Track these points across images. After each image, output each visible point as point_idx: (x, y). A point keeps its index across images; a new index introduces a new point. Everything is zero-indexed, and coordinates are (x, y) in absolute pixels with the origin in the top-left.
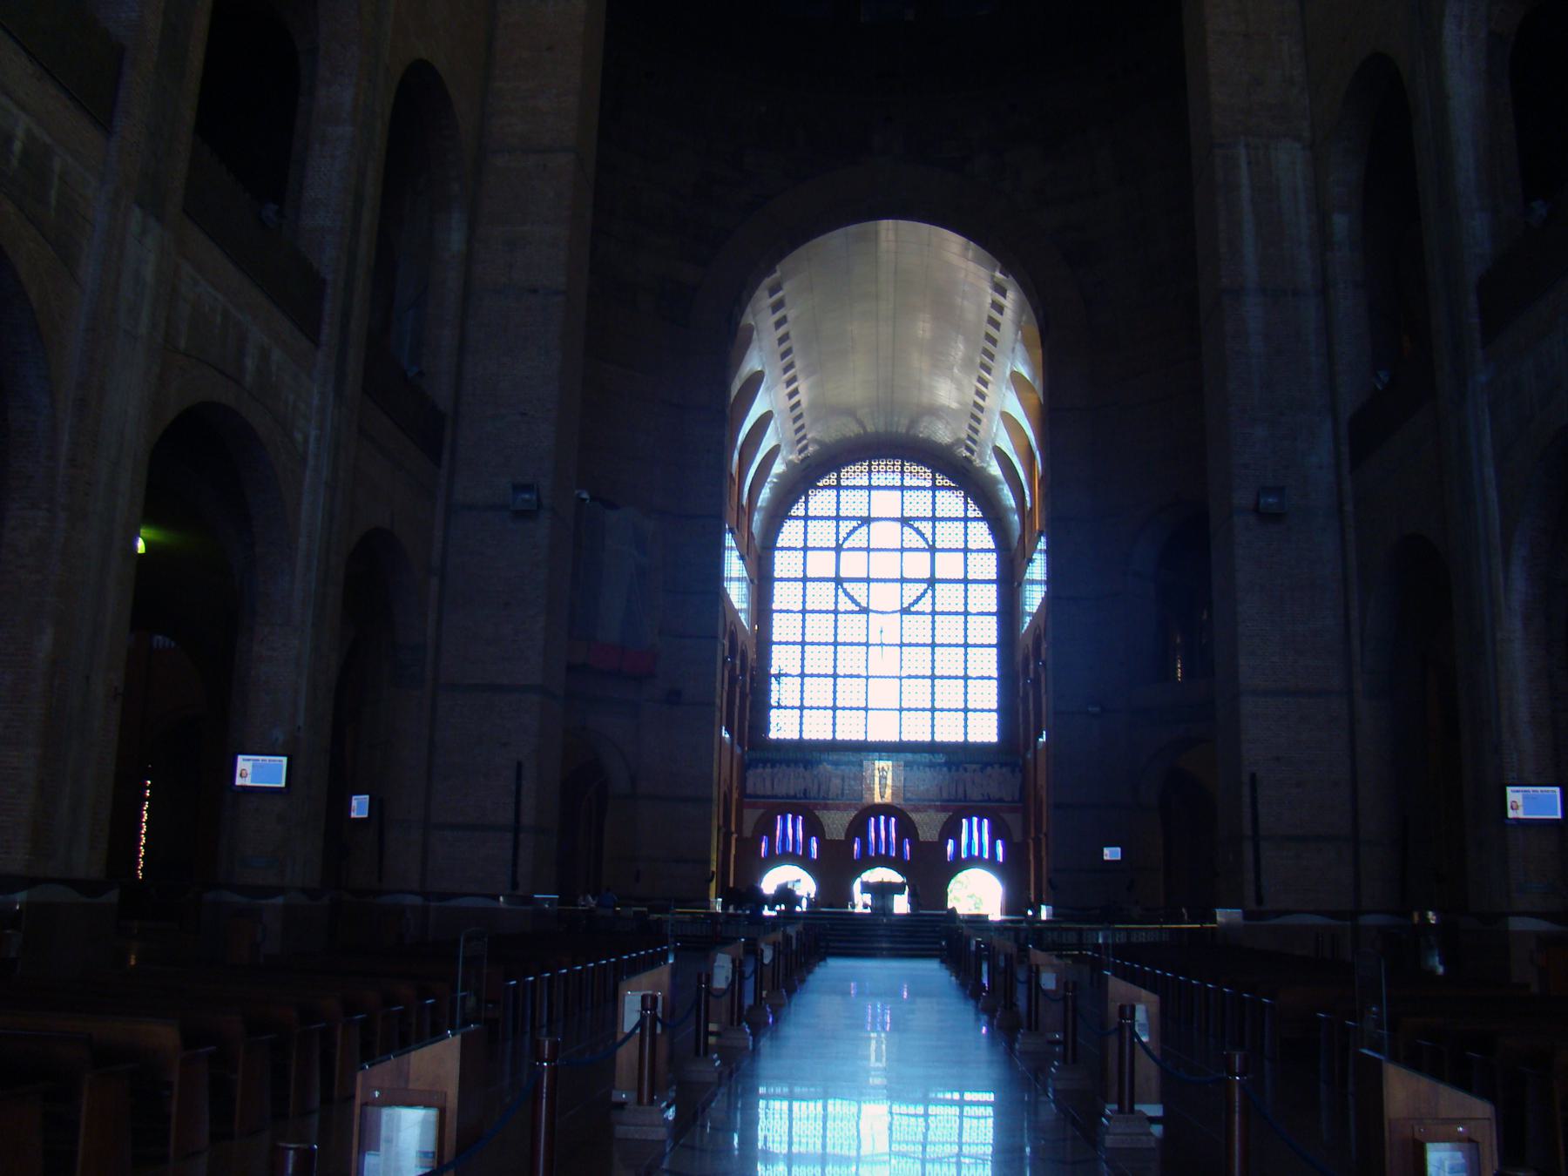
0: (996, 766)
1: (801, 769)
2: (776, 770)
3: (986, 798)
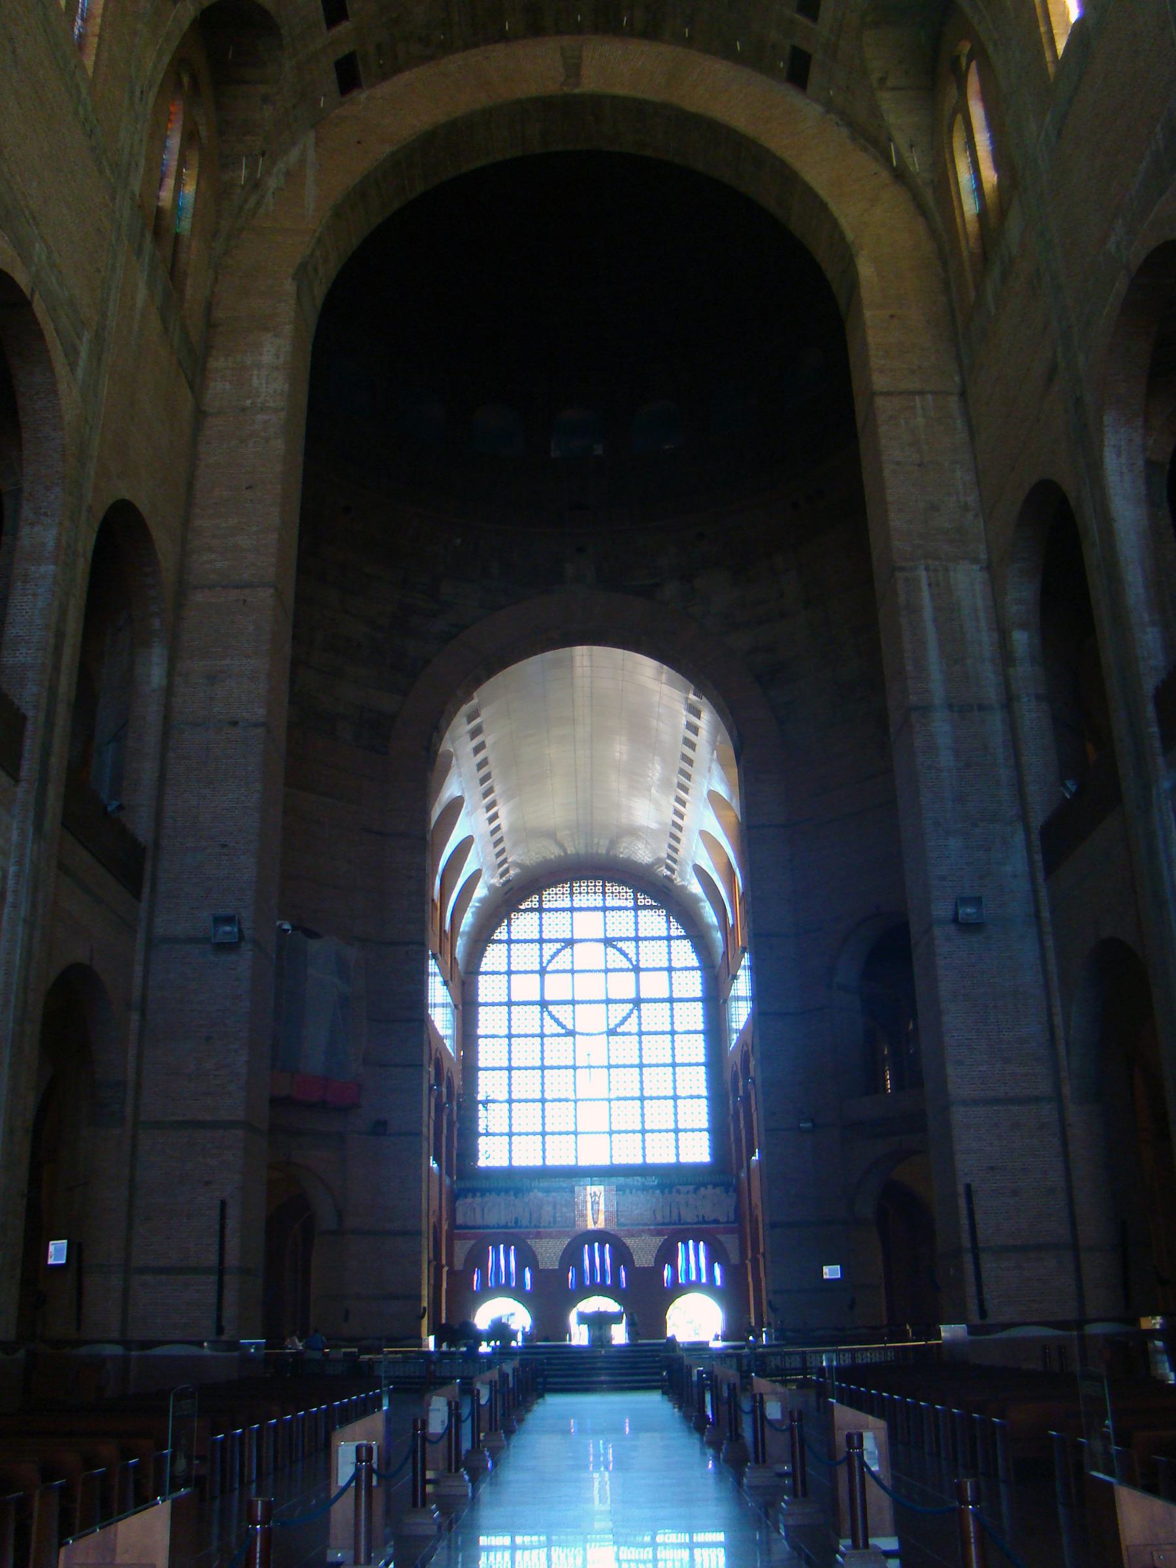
0: (710, 1187)
2: (485, 1199)
3: (701, 1218)
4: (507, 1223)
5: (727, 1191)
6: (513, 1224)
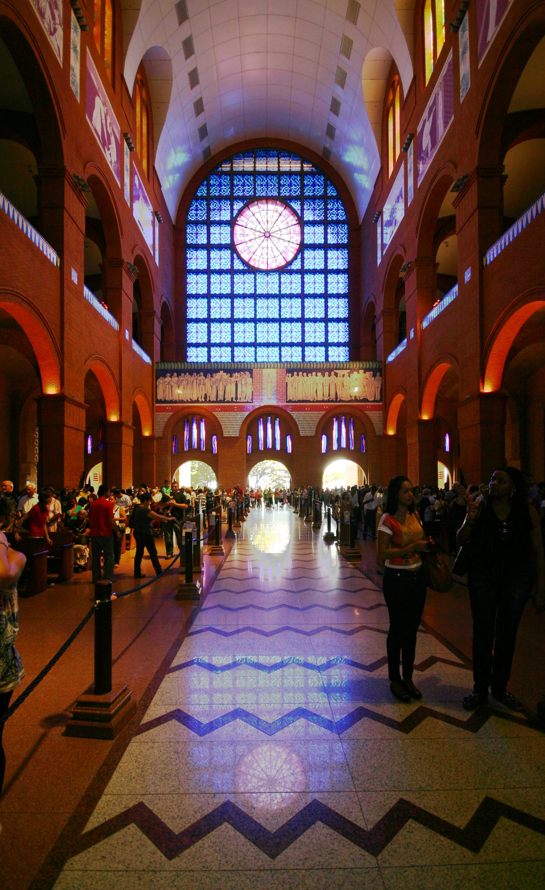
0: (361, 371)
1: (203, 377)
2: (181, 378)
4: (198, 398)
5: (374, 376)
6: (204, 400)
